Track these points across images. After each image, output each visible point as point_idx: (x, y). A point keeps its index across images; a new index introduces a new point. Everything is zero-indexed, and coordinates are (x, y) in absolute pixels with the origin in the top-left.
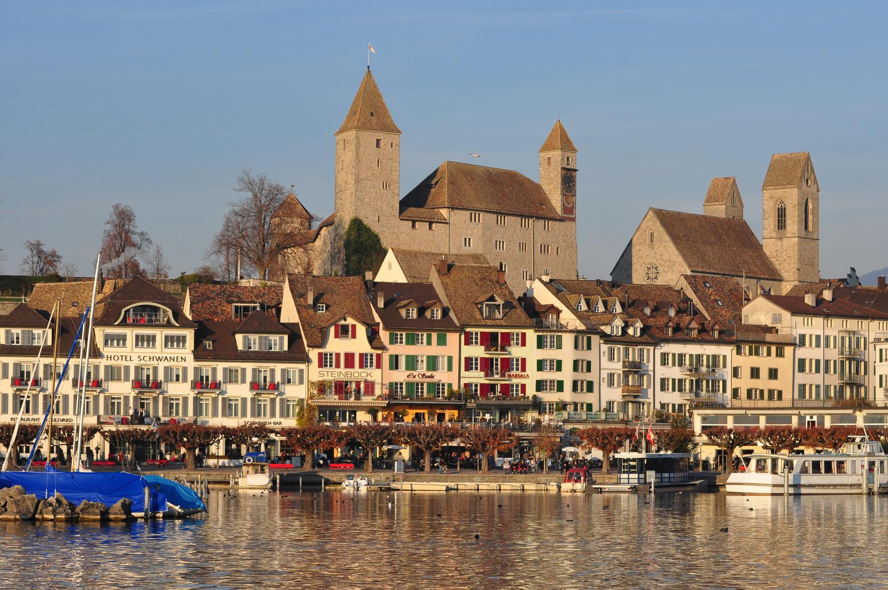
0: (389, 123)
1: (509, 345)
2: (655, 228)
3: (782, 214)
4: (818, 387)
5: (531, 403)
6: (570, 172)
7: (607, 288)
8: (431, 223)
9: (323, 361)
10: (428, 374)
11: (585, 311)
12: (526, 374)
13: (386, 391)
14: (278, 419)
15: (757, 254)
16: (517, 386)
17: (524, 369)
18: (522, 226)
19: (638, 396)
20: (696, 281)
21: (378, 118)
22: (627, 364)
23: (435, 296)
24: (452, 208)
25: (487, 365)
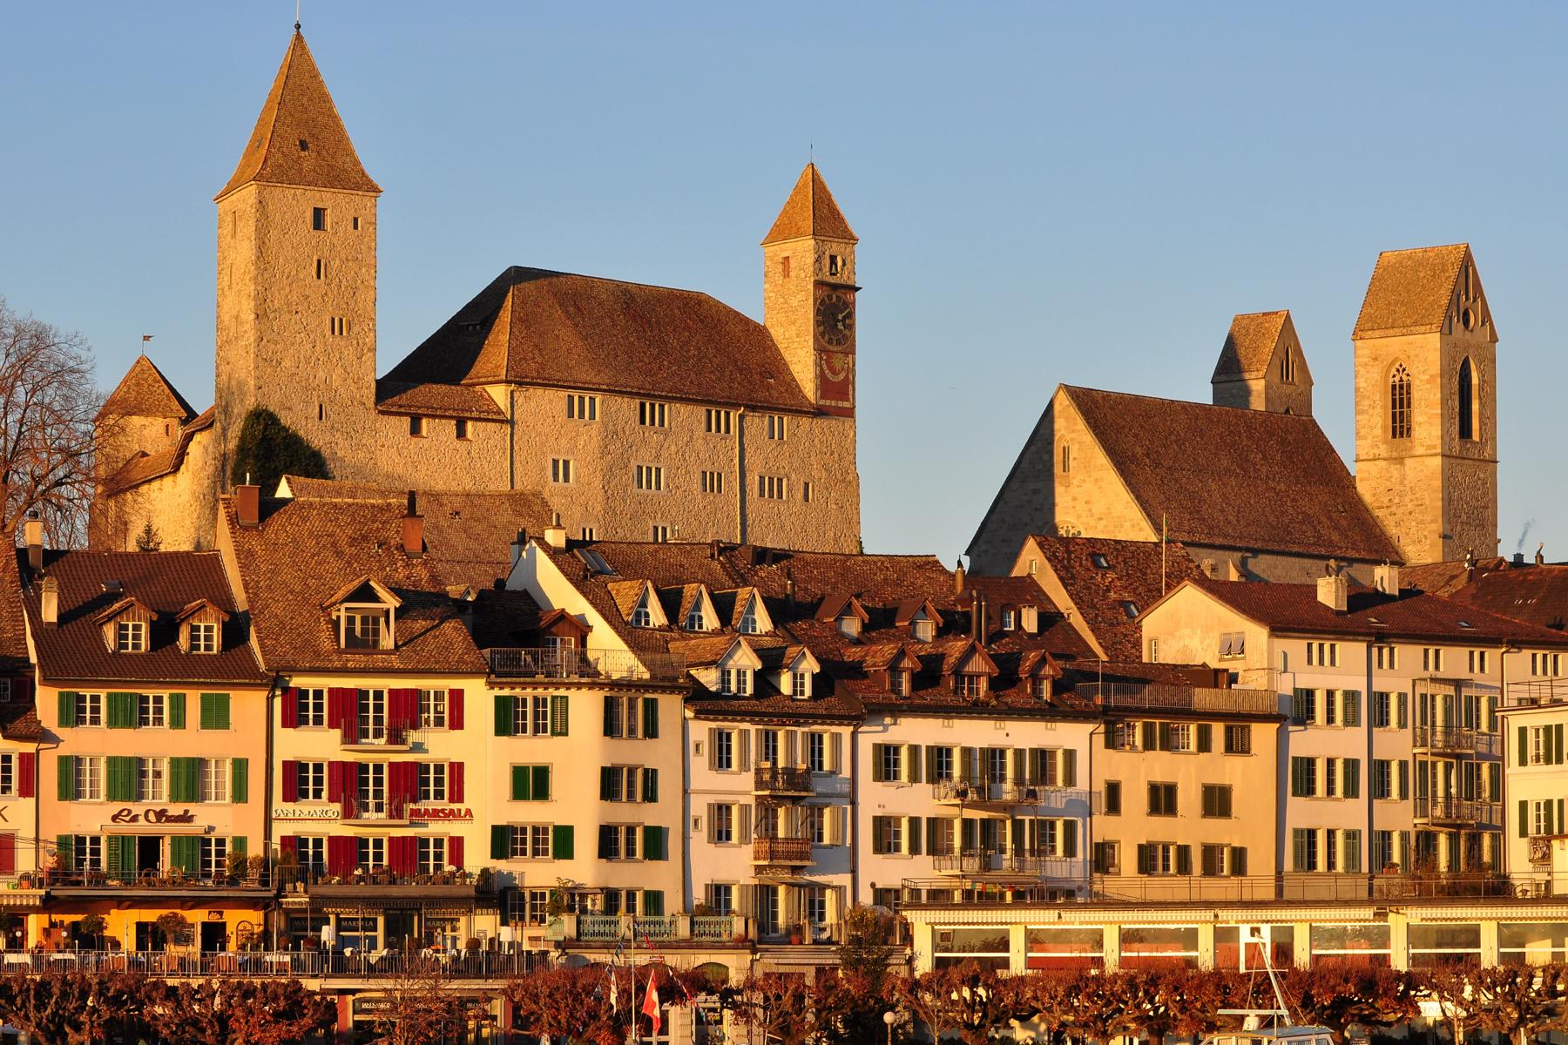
0: (349, 166)
1: (415, 726)
4: (1352, 836)
5: (472, 892)
6: (840, 293)
10: (176, 809)
11: (661, 629)
12: (463, 807)
13: (49, 862)
15: (1340, 500)
17: (458, 796)
19: (805, 866)
21: (319, 154)
22: (766, 777)
24: (520, 384)
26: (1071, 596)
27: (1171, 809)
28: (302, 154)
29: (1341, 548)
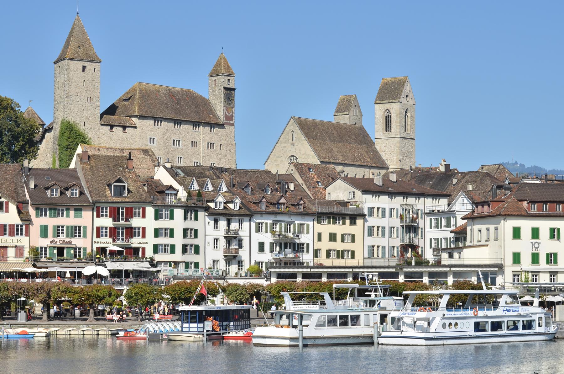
2: (296, 131)
3: (388, 121)
8: (124, 128)
17: (144, 236)
18: (193, 129)
19: (237, 256)
20: (302, 167)
23: (78, 178)
25: (113, 233)
26: (303, 180)
27: (335, 240)
28: (79, 50)
29: (371, 163)
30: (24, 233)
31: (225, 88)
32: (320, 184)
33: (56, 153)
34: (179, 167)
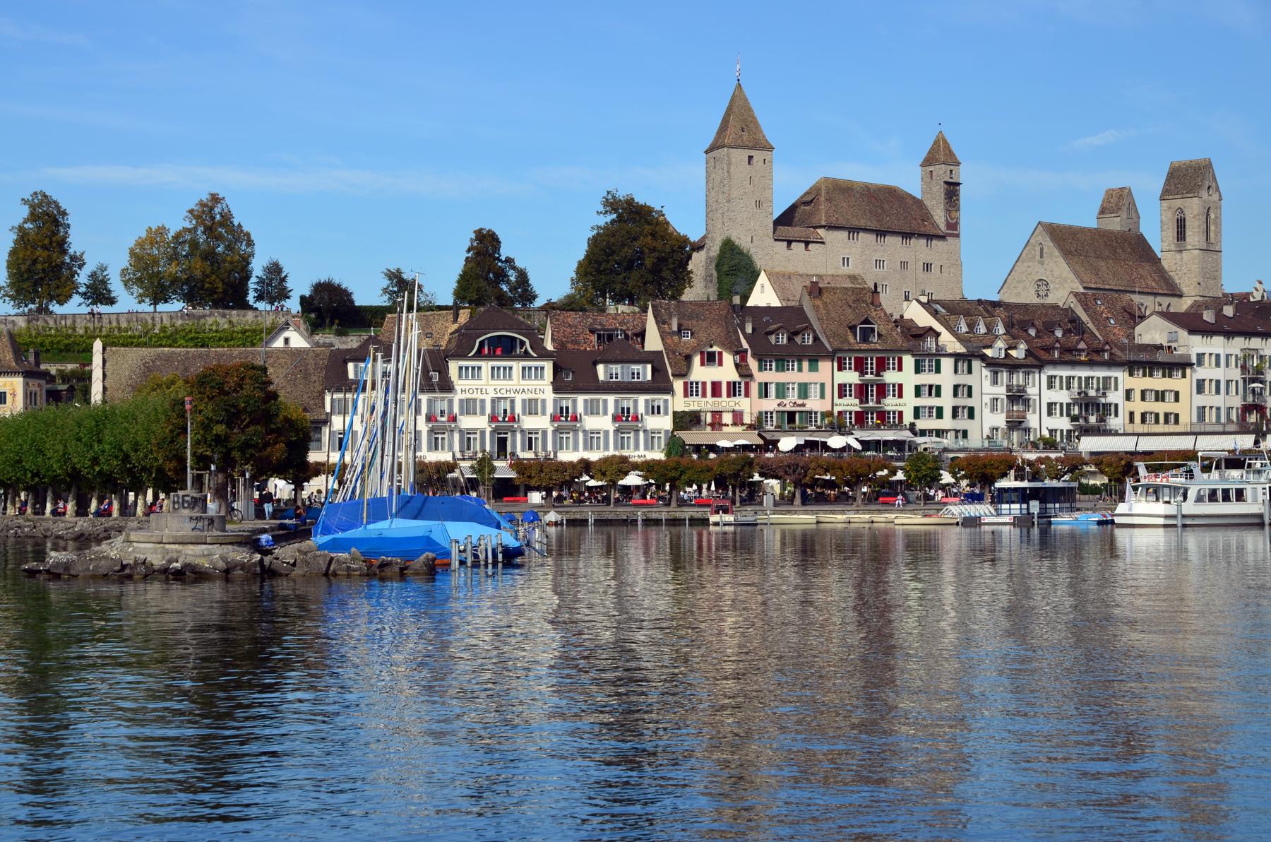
4: (1218, 409)
7: (989, 308)
8: (807, 243)
9: (689, 390)
10: (800, 402)
14: (642, 452)
16: (894, 413)
17: (900, 396)
23: (806, 319)
25: (862, 391)
30: (743, 393)
31: (946, 183)
32: (1112, 322)
33: (711, 281)
34: (937, 302)
